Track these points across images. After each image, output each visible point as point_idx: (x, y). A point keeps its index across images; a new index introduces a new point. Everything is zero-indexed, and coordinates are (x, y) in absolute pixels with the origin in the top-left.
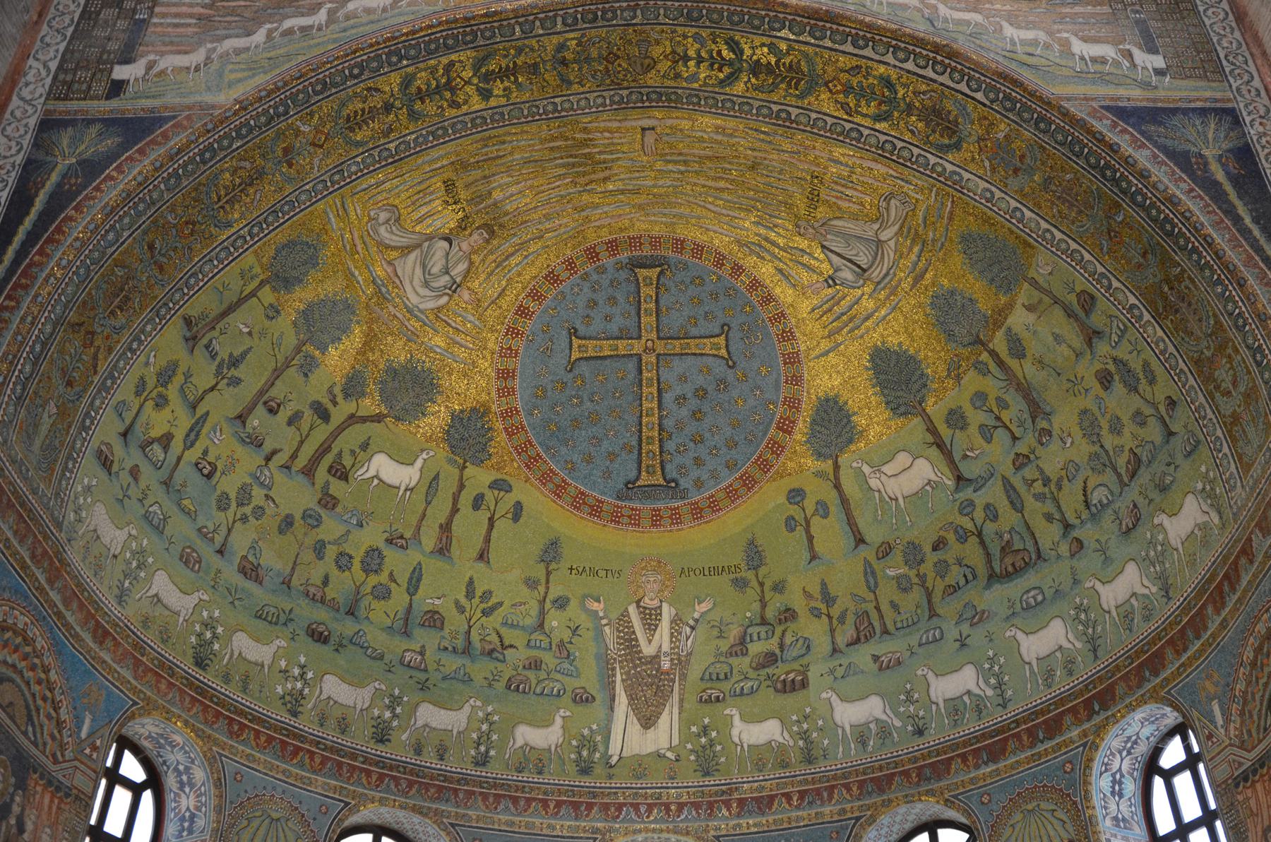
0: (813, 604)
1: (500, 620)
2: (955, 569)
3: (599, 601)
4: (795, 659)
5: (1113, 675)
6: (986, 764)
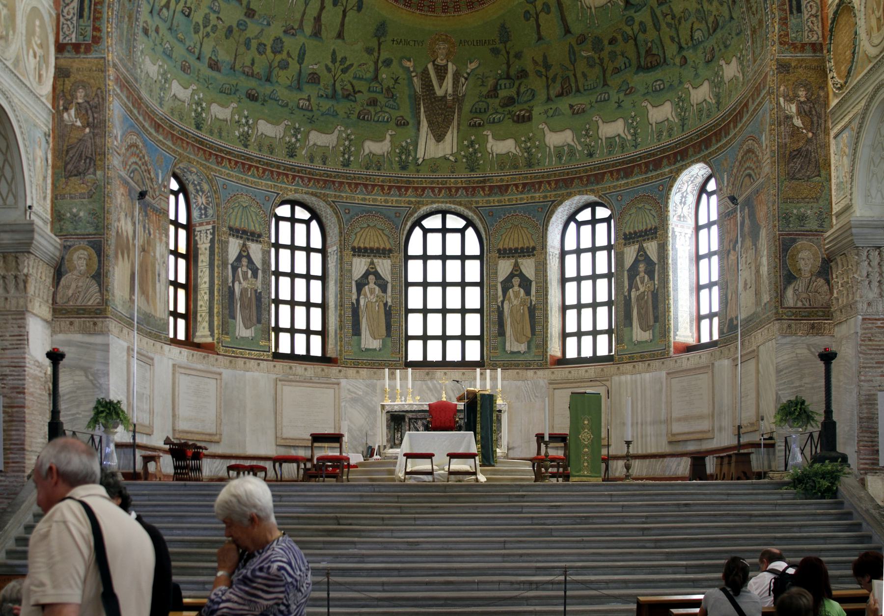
0: (538, 68)
1: (352, 75)
2: (620, 58)
3: (409, 60)
4: (526, 102)
5: (689, 143)
6: (622, 179)
